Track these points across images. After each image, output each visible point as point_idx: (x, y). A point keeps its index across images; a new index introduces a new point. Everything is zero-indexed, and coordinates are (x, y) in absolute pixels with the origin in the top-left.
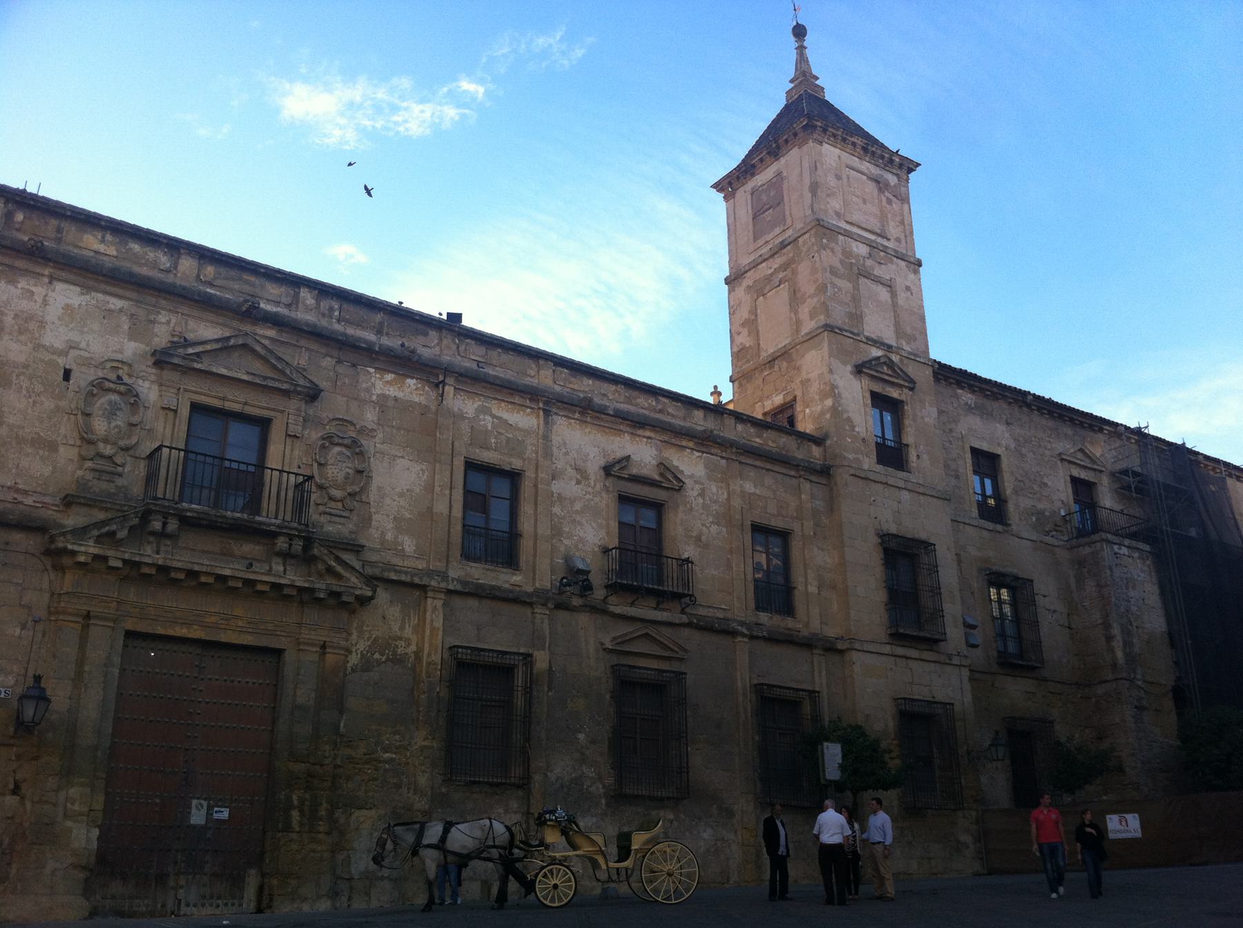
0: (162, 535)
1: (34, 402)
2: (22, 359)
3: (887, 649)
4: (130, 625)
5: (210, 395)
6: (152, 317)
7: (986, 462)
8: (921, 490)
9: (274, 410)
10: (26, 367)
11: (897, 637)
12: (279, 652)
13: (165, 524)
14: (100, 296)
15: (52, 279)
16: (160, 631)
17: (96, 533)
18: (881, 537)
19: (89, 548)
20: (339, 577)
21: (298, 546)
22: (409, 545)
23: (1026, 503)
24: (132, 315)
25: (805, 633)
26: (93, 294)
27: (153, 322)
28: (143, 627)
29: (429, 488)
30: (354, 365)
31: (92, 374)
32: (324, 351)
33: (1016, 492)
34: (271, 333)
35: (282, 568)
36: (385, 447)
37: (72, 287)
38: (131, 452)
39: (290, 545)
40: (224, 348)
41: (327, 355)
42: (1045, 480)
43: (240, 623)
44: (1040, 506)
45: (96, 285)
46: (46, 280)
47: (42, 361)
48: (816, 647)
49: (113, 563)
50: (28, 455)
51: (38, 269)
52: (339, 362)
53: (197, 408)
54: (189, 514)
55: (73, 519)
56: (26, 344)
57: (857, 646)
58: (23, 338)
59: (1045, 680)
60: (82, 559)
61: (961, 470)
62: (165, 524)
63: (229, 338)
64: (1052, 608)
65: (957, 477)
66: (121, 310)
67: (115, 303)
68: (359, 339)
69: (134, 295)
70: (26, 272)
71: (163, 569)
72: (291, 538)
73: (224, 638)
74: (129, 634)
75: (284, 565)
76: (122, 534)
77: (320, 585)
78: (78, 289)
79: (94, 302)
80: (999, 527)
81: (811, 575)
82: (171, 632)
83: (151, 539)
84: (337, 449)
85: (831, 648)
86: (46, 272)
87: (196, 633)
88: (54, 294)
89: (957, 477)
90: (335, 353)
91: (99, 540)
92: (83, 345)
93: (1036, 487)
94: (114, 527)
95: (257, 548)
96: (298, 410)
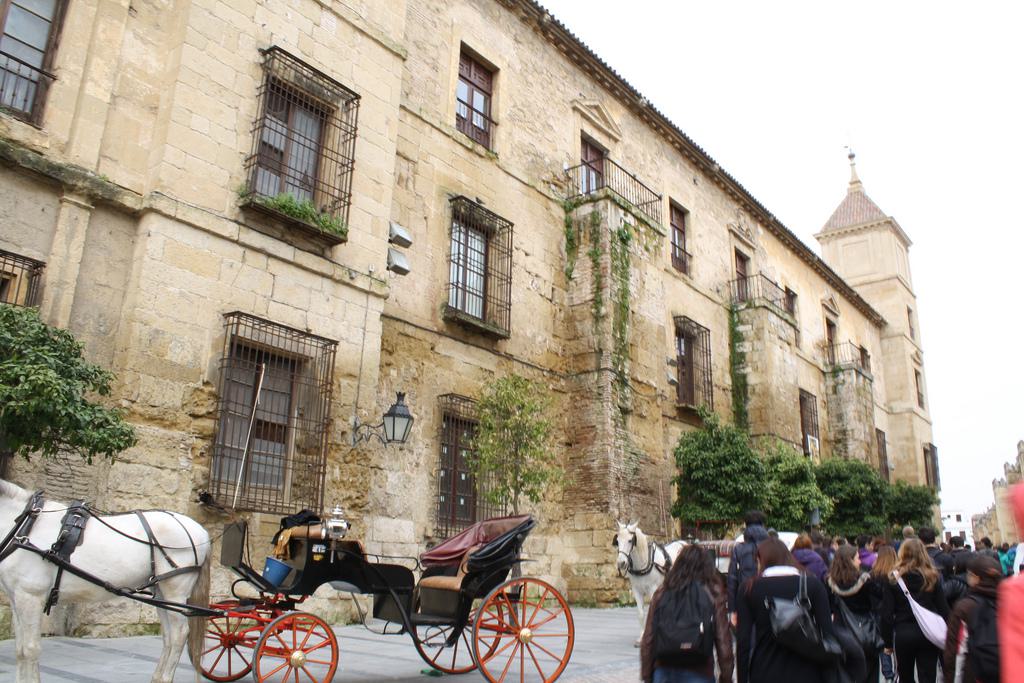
3: (231, 229)
7: (478, 68)
8: (360, 24)
11: (257, 214)
18: (264, 53)
23: (522, 137)
25: (57, 159)
33: (512, 119)
42: (551, 122)
44: (540, 148)
48: (72, 189)
57: (160, 205)
59: (509, 357)
61: (442, 62)
64: (534, 271)
65: (435, 68)
80: (480, 149)
81: (99, 67)
85: (105, 202)
89: (435, 68)
93: (537, 124)
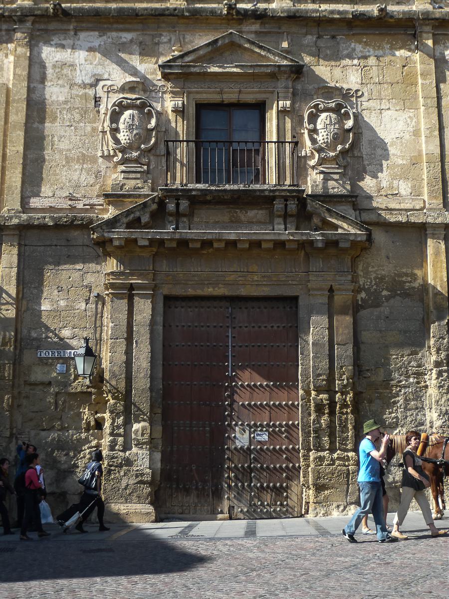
0: (178, 214)
1: (76, 128)
2: (62, 99)
4: (166, 290)
5: (210, 95)
6: (156, 40)
9: (265, 92)
10: (66, 102)
12: (295, 299)
13: (178, 205)
14: (114, 34)
15: (76, 31)
16: (191, 292)
17: (125, 220)
19: (119, 234)
20: (336, 227)
21: (293, 206)
22: (404, 188)
24: (141, 43)
26: (109, 34)
27: (158, 44)
28: (178, 291)
29: (416, 133)
30: (333, 37)
31: (115, 98)
32: (304, 31)
34: (256, 27)
35: (283, 227)
36: (371, 104)
37: (92, 33)
38: (153, 151)
39: (286, 205)
40: (215, 51)
41: (306, 34)
43: (256, 278)
45: (110, 26)
46: (72, 33)
47: (77, 96)
49: (141, 243)
50: (76, 170)
51: (65, 27)
52: (319, 37)
53: (201, 108)
54: (194, 193)
55: (111, 212)
56: (64, 86)
58: (60, 82)
60: (116, 243)
62: (178, 205)
63: (216, 41)
66: (131, 41)
67: (127, 36)
68: (332, 12)
69: (140, 26)
70: (55, 32)
71: (183, 243)
72: (286, 199)
73: (243, 292)
74: (168, 299)
75: (285, 224)
76: (145, 219)
77: (317, 236)
78: (97, 33)
79: (110, 40)
82: (199, 292)
83: (171, 219)
84: (324, 115)
86: (71, 27)
87: (221, 291)
88: (79, 43)
90: (315, 30)
91: (129, 226)
92: (106, 76)
94: (138, 214)
95: (260, 212)
96: (286, 87)
